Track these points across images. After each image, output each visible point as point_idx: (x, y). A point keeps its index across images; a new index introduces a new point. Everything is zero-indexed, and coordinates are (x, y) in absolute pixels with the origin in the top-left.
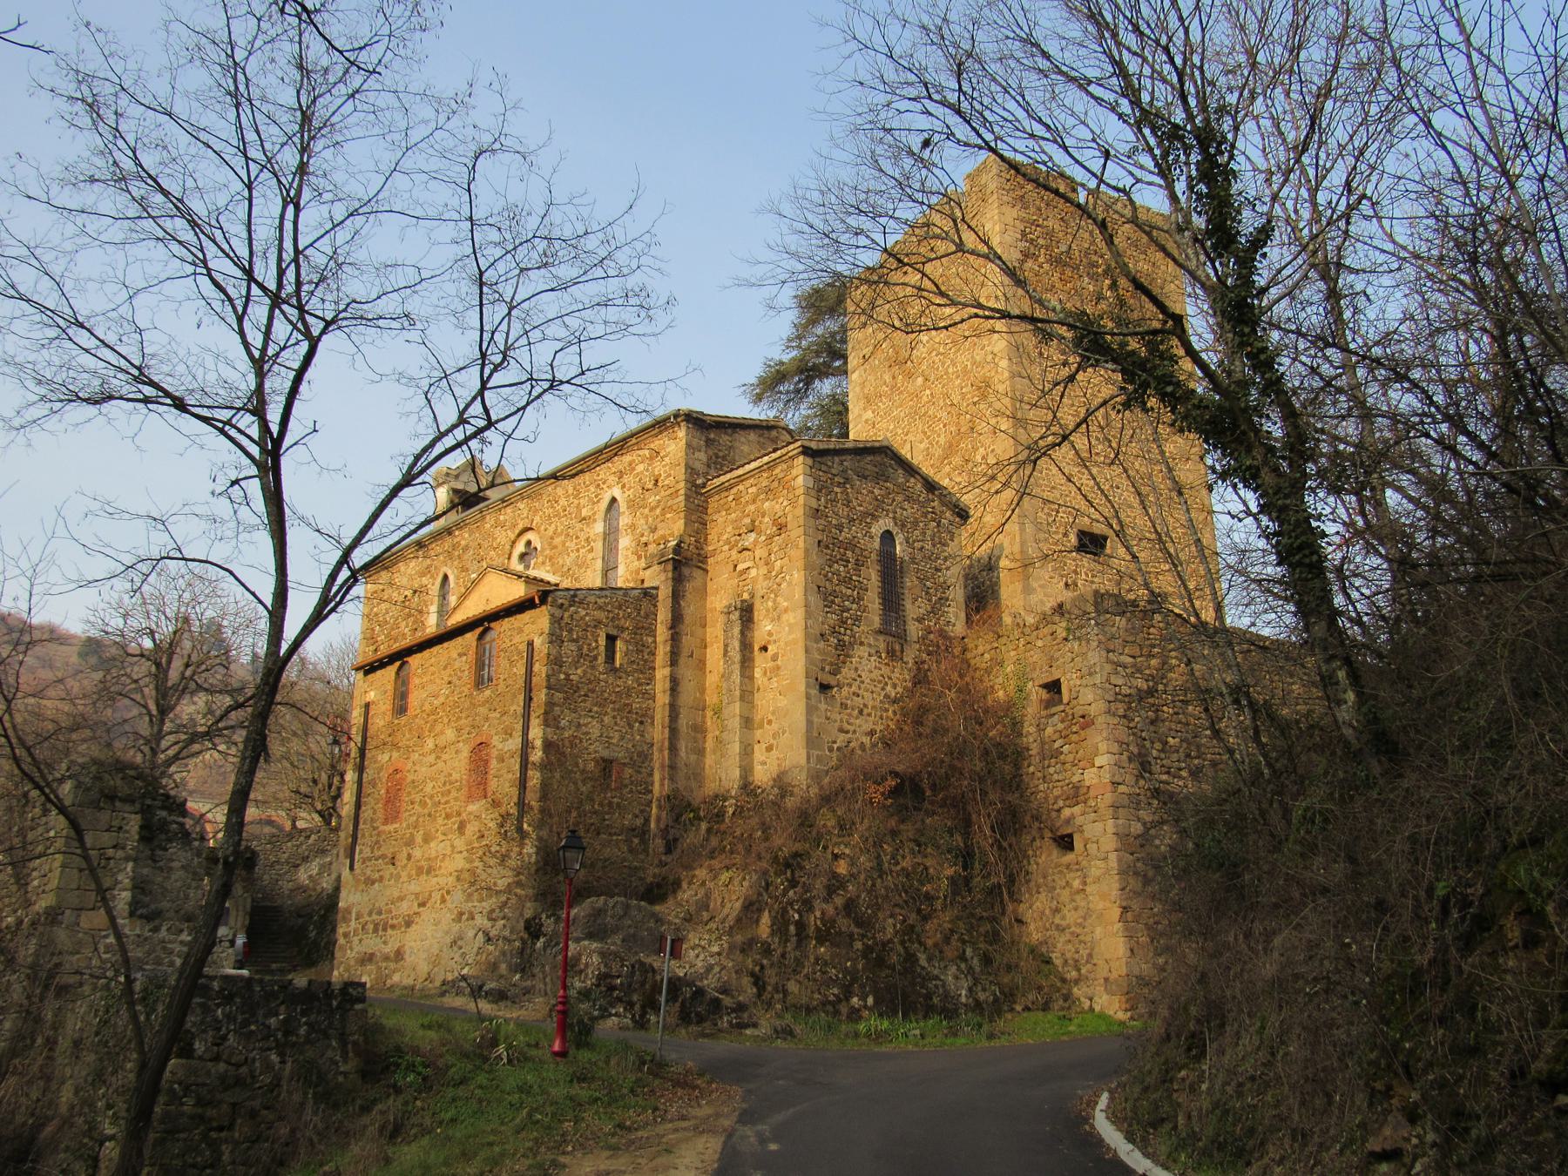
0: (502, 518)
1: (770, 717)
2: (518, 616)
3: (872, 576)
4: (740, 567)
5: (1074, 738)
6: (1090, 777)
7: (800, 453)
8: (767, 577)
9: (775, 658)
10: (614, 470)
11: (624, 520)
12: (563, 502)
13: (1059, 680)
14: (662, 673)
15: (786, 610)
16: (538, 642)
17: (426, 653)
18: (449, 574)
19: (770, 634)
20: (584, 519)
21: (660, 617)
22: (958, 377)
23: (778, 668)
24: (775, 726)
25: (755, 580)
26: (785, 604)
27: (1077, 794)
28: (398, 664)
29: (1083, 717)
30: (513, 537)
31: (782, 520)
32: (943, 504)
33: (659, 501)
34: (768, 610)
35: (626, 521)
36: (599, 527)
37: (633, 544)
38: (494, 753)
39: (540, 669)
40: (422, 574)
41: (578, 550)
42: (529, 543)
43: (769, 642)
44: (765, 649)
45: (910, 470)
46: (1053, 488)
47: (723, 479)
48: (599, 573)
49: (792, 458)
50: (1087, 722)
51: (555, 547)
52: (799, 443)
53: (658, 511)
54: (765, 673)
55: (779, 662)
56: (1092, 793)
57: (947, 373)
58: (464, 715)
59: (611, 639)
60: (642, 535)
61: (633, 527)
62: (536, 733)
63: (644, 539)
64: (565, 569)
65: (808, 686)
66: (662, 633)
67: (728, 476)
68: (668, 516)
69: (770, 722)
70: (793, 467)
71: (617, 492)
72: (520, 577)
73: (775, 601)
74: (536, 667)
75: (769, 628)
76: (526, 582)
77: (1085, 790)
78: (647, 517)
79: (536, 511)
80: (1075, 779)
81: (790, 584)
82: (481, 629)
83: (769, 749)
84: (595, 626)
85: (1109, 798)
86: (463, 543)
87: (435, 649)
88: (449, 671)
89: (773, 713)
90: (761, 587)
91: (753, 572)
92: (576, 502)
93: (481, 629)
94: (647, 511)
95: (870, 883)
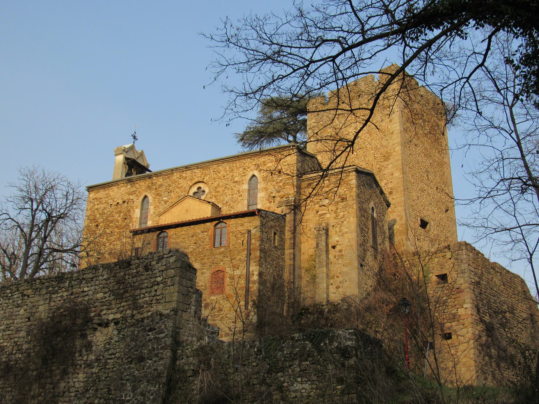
0: (184, 175)
1: (338, 275)
2: (241, 219)
3: (370, 223)
4: (320, 213)
5: (453, 296)
6: (461, 311)
7: (353, 171)
8: (335, 218)
9: (340, 251)
10: (254, 163)
11: (260, 186)
12: (223, 173)
13: (446, 274)
14: (288, 252)
15: (346, 233)
16: (253, 231)
17: (179, 229)
18: (149, 195)
19: (338, 241)
20: (236, 182)
21: (287, 228)
22: (372, 150)
23: (342, 255)
24: (341, 279)
25: (328, 219)
26: (346, 230)
27: (455, 317)
28: (159, 232)
29: (458, 289)
30: (191, 184)
31: (344, 196)
32: (384, 200)
33: (281, 180)
34: (336, 232)
35: (262, 186)
36: (246, 187)
37: (267, 196)
38: (227, 275)
39: (256, 243)
40: (130, 194)
41: (232, 195)
42: (199, 188)
43: (337, 245)
44: (334, 247)
45: (378, 185)
46: (414, 200)
47: (312, 175)
48: (246, 206)
49: (350, 172)
50: (459, 290)
51: (218, 192)
52: (355, 167)
53: (281, 184)
54: (335, 257)
55: (343, 253)
56: (462, 317)
57: (366, 147)
58: (206, 258)
59: (275, 234)
60: (272, 193)
61: (266, 189)
62: (254, 269)
63: (273, 195)
64: (225, 202)
65: (358, 264)
66: (288, 235)
67: (315, 175)
68: (287, 187)
69: (338, 277)
70: (349, 176)
71: (256, 173)
72: (209, 202)
73: (340, 228)
74: (253, 241)
75: (337, 239)
76: (212, 205)
77: (458, 316)
78: (274, 185)
79: (206, 175)
80: (454, 311)
81: (348, 222)
82: (217, 222)
83: (338, 287)
84: (271, 228)
85: (470, 320)
86: (159, 183)
87: (185, 228)
88: (195, 238)
89: (340, 273)
90: (332, 222)
91: (328, 216)
92: (231, 174)
93: (217, 222)
94: (274, 183)
95: (389, 343)
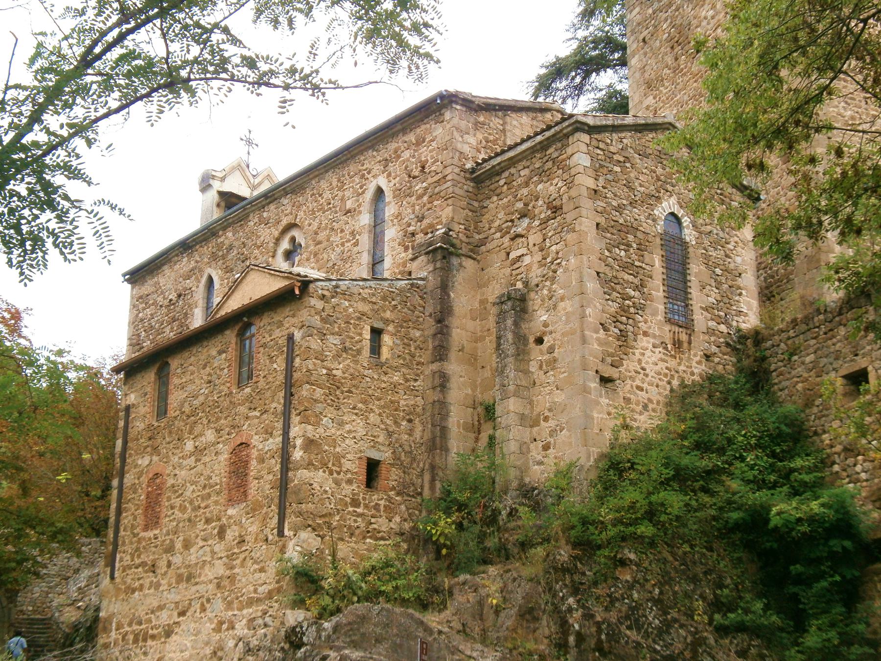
0: (265, 215)
3: (656, 262)
4: (513, 255)
8: (541, 264)
10: (379, 158)
11: (390, 210)
12: (327, 195)
19: (546, 325)
20: (349, 211)
25: (529, 267)
30: (276, 234)
31: (557, 203)
33: (426, 189)
36: (365, 219)
38: (254, 453)
41: (343, 245)
42: (293, 239)
43: (544, 333)
44: (540, 341)
49: (567, 136)
51: (320, 243)
54: (541, 367)
59: (376, 333)
60: (409, 225)
61: (399, 216)
63: (411, 228)
64: (330, 264)
68: (436, 203)
70: (568, 145)
71: (382, 182)
73: (550, 290)
75: (544, 318)
82: (240, 324)
83: (546, 447)
84: (359, 319)
86: (227, 242)
89: (550, 410)
91: (527, 260)
93: (240, 324)
